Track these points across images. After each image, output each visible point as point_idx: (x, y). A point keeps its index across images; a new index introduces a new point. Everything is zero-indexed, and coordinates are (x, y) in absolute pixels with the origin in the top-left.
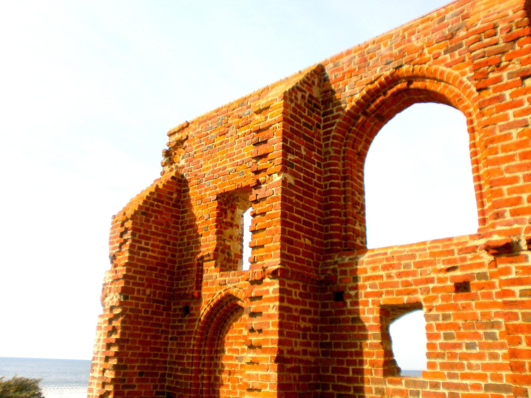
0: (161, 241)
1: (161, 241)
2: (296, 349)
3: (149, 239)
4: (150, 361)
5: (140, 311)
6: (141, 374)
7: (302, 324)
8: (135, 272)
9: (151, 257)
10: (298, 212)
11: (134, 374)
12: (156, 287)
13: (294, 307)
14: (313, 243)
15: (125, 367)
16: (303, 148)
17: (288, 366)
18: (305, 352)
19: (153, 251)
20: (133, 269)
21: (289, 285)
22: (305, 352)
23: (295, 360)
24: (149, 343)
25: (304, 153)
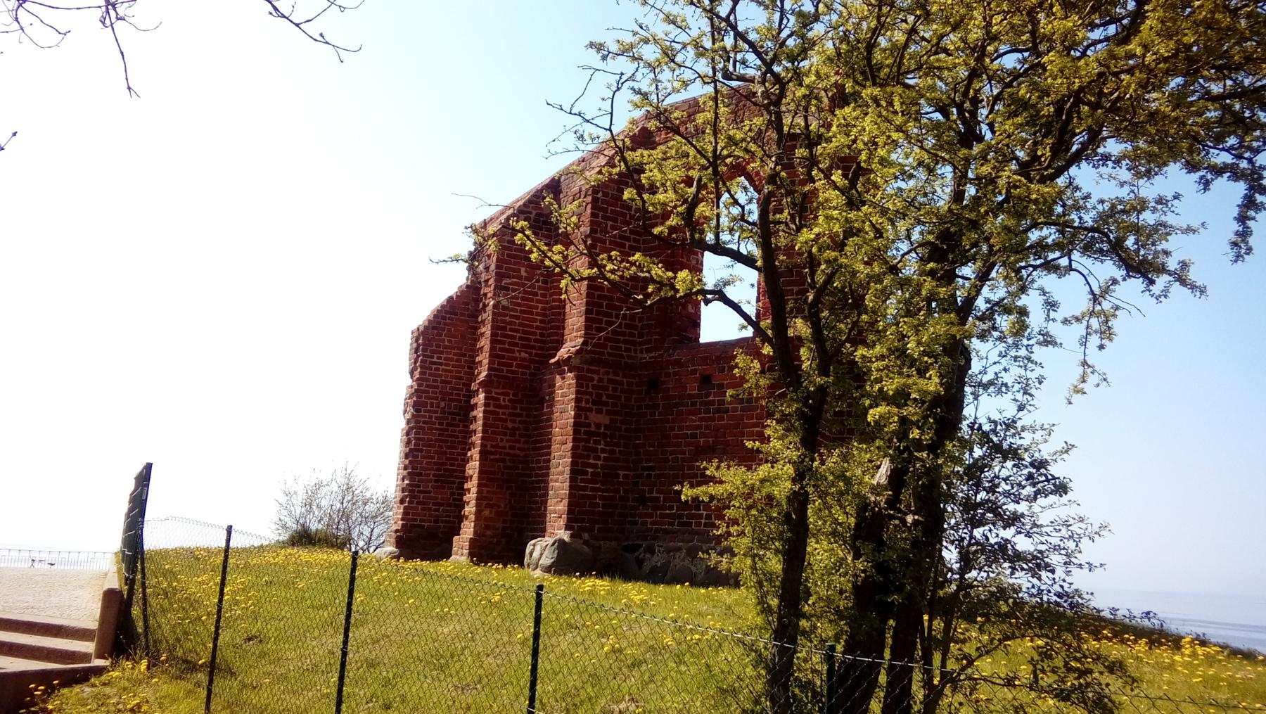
0: (454, 354)
1: (454, 354)
2: (501, 444)
3: (442, 353)
4: (446, 470)
5: (434, 423)
6: (436, 481)
7: (510, 425)
8: (427, 386)
9: (443, 370)
10: (511, 330)
11: (430, 481)
12: (450, 399)
13: (501, 411)
14: (530, 354)
15: (420, 474)
16: (523, 270)
17: (492, 457)
18: (512, 448)
19: (446, 365)
20: (425, 383)
21: (496, 393)
22: (512, 448)
23: (501, 453)
24: (445, 453)
25: (523, 274)
